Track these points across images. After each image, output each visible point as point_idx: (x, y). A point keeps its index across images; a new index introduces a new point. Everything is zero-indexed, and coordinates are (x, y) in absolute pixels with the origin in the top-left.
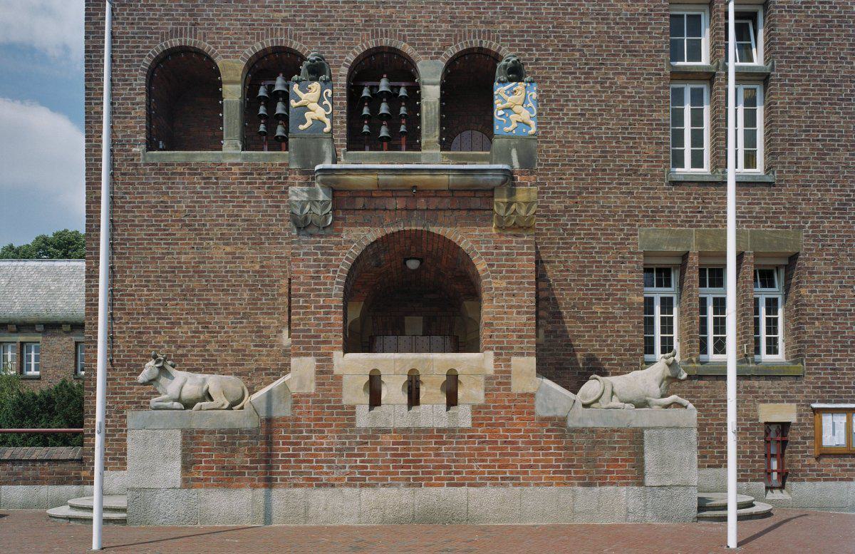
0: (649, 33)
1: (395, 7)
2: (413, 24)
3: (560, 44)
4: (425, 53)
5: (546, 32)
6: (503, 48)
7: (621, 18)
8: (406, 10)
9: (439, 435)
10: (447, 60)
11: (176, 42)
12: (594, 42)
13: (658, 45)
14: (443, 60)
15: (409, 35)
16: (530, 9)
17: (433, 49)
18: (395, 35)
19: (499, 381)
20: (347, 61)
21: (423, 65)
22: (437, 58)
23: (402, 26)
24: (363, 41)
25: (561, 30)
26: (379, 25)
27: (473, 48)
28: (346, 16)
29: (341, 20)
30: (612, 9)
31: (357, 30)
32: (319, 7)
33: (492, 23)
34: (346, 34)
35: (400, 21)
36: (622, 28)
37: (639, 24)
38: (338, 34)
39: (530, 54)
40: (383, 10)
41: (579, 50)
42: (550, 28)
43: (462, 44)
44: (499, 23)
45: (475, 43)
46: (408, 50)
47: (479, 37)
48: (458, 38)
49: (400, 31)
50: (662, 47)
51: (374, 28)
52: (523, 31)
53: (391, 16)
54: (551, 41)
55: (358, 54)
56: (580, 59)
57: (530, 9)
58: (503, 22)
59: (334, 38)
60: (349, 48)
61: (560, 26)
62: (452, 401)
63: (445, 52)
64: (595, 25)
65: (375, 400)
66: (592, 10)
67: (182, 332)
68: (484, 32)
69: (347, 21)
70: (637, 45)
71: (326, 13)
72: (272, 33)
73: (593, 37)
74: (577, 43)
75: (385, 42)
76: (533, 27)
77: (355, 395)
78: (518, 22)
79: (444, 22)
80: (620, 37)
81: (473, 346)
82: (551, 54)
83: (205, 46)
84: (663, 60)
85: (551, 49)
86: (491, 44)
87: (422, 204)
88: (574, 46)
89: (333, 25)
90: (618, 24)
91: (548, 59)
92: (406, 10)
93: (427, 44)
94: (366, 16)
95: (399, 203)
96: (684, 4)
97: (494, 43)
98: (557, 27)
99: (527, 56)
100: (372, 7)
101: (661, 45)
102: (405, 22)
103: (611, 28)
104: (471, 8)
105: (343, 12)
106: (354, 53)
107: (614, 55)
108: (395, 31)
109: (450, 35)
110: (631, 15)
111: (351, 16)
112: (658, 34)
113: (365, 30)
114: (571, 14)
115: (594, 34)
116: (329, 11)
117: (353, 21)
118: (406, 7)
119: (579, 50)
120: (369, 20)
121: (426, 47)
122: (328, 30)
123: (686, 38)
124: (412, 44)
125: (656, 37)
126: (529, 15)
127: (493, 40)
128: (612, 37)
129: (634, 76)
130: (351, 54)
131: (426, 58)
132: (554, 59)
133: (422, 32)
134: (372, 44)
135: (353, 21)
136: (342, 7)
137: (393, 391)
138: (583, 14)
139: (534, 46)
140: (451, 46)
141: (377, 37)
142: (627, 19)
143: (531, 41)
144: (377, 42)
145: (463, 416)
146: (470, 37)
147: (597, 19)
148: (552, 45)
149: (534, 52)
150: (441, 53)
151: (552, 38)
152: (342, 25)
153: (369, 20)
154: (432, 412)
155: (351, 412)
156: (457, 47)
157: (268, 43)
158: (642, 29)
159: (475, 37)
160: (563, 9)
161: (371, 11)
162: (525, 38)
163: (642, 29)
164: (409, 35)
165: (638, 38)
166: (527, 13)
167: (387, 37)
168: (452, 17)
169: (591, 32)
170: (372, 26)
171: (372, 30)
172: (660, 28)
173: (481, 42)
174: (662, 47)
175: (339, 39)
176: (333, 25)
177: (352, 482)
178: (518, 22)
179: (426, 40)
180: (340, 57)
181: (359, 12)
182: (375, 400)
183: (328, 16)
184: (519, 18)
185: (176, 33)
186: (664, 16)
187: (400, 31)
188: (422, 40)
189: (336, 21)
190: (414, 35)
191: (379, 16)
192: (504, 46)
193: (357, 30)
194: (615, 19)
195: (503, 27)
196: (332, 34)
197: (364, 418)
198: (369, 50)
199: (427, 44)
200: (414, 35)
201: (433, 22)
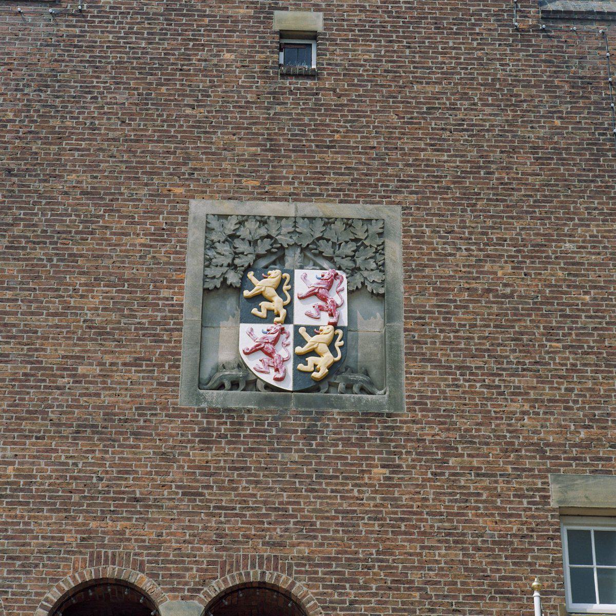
0: (530, 564)
1: (129, 519)
2: (157, 545)
3: (389, 579)
4: (173, 590)
5: (366, 560)
6: (298, 584)
7: (484, 542)
8: (147, 523)
10: (208, 600)
12: (443, 576)
13: (546, 584)
14: (201, 601)
15: (149, 562)
16: (342, 525)
17: (186, 584)
18: (128, 561)
20: (47, 600)
21: (168, 609)
22: (192, 598)
23: (139, 547)
24: (75, 570)
25: (391, 558)
26: (103, 546)
27: (251, 583)
28: (52, 531)
29: (43, 537)
30: (470, 528)
31: (68, 552)
32: (10, 517)
33: (281, 545)
34: (49, 559)
35: (136, 540)
36: (488, 556)
37: (514, 550)
38: (36, 558)
39: (340, 594)
40: (110, 523)
41: (419, 589)
42: (372, 554)
43: (233, 577)
44: (293, 545)
45: (254, 575)
46: (145, 583)
47: (261, 567)
48: (228, 568)
49: (135, 554)
50: (552, 586)
51: (96, 550)
52: (329, 558)
53: (122, 533)
54: (374, 574)
55: (66, 589)
56: (420, 603)
57: (342, 525)
58: (299, 544)
59: (30, 565)
60: (52, 580)
61: (388, 551)
63: (205, 589)
64: (443, 552)
66: (439, 528)
68: (268, 558)
69: (53, 538)
70: (512, 583)
71: (21, 527)
73: (442, 569)
74: (415, 577)
75: (111, 571)
76: (346, 552)
78: (322, 545)
79: (205, 542)
80: (484, 571)
82: (375, 595)
84: (555, 607)
85: (374, 586)
86: (278, 577)
88: (412, 582)
89: (29, 544)
90: (479, 549)
91: (369, 602)
92: (147, 523)
93: (178, 576)
94: (84, 532)
96: (582, 516)
97: (284, 576)
98: (384, 553)
99: (336, 597)
100: (95, 518)
101: (550, 583)
102: (144, 541)
103: (468, 555)
104: (248, 522)
105: (48, 525)
106: (59, 588)
107: (474, 597)
108: (128, 554)
109: (214, 563)
110: (500, 536)
111: (60, 531)
112: (544, 566)
113: (81, 553)
114: (405, 533)
115: (443, 565)
116: (26, 524)
117: (62, 539)
118: (148, 519)
119: (419, 589)
120: (87, 537)
121: (176, 580)
122: (21, 551)
123: (595, 566)
124: (153, 576)
125: (542, 571)
126: (341, 534)
127: (283, 571)
128: (471, 570)
130: (55, 589)
131: (175, 598)
132: (379, 602)
133: (171, 558)
134: (89, 574)
135: (62, 539)
136: (46, 518)
138: (424, 533)
139: (347, 581)
140: (215, 578)
141: (99, 563)
142: (494, 542)
143: (343, 573)
144: (97, 571)
146: (246, 566)
147: (447, 541)
148: (376, 580)
149: (348, 590)
150: (199, 590)
151: (376, 570)
152: (44, 545)
153: (87, 537)
156: (225, 581)
158: (519, 558)
159: (253, 566)
160: (393, 526)
161: (93, 525)
162: (333, 569)
164: (149, 562)
165: (513, 571)
166: (337, 531)
167: (114, 564)
168: (220, 536)
169: (437, 562)
170: (92, 546)
171: (92, 554)
172: (547, 558)
173: (263, 574)
174: (552, 586)
175: (37, 566)
176: (29, 544)
178: (322, 545)
179: (177, 569)
180: (37, 594)
181: (72, 525)
183: (22, 531)
184: (324, 538)
186: (552, 539)
187: (135, 554)
188: (169, 569)
189: (37, 538)
190: (157, 562)
191: (103, 532)
192: (300, 581)
193: (68, 552)
194: (475, 542)
195: (299, 552)
196: (27, 558)
198: (85, 583)
199: (178, 576)
200: (157, 562)
201: (189, 543)
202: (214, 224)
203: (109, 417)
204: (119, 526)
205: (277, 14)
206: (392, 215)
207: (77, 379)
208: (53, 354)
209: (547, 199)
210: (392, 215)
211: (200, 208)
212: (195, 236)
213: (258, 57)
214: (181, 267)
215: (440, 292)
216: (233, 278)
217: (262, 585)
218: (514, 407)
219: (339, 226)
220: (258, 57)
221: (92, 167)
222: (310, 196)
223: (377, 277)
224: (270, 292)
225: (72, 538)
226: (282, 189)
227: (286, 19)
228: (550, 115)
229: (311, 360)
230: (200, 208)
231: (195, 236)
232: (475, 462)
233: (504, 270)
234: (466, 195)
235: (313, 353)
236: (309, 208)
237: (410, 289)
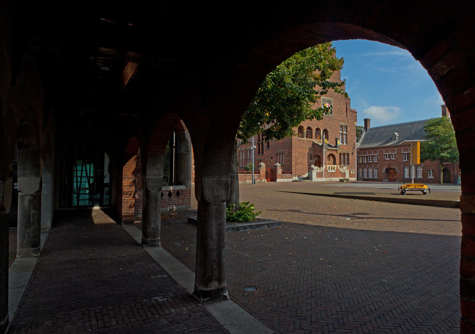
9: (334, 173)
19: (337, 168)
46: (320, 128)
62: (334, 170)
65: (329, 170)
75: (318, 127)
77: (328, 169)
81: (336, 165)
83: (303, 126)
87: (332, 151)
95: (331, 151)
120: (317, 124)
134: (317, 127)
137: (330, 169)
145: (335, 171)
154: (333, 171)
155: (328, 170)
157: (309, 126)
177: (328, 177)
182: (329, 170)
197: (329, 171)
210: (332, 99)
212: (322, 100)
218: (338, 117)
222: (328, 97)
225: (316, 124)
231: (322, 100)
233: (338, 105)
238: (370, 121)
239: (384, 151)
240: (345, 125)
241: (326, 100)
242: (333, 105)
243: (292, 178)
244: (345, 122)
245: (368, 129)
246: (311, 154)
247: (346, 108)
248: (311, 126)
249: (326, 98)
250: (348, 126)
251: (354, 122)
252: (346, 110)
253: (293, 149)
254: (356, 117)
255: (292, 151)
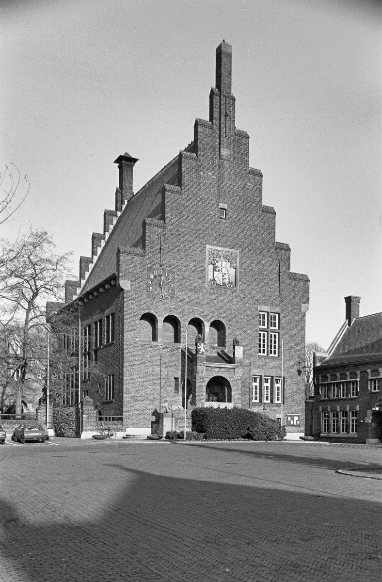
2: (203, 312)
11: (147, 311)
46: (202, 319)
67: (148, 390)
72: (171, 311)
75: (197, 316)
120: (193, 309)
129: (251, 330)
158: (253, 318)
163: (253, 318)
185: (148, 309)
202: (210, 250)
203: (195, 288)
204: (197, 308)
205: (220, 204)
206: (238, 252)
207: (190, 280)
208: (186, 274)
209: (261, 252)
210: (238, 252)
211: (208, 247)
212: (207, 253)
213: (217, 213)
214: (205, 259)
215: (245, 269)
216: (213, 263)
217: (218, 320)
219: (230, 253)
220: (217, 213)
221: (190, 235)
222: (225, 247)
223: (235, 265)
224: (219, 266)
225: (191, 310)
226: (220, 244)
227: (221, 205)
228: (262, 234)
229: (225, 280)
230: (208, 247)
232: (248, 301)
234: (249, 249)
235: (225, 279)
236: (225, 249)
237: (240, 268)
238: (359, 302)
239: (369, 371)
240: (272, 311)
241: (220, 253)
242: (241, 264)
243: (122, 430)
244: (273, 305)
245: (352, 322)
246: (176, 377)
247: (276, 272)
248: (176, 315)
249: (218, 248)
250: (281, 315)
251: (299, 305)
252: (276, 275)
253: (125, 365)
254: (306, 291)
255: (125, 370)
